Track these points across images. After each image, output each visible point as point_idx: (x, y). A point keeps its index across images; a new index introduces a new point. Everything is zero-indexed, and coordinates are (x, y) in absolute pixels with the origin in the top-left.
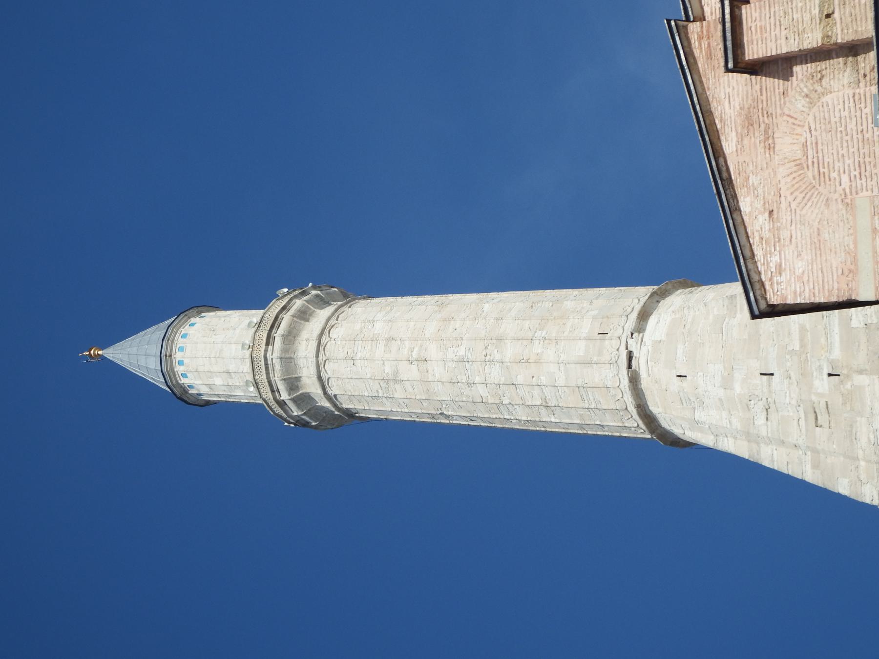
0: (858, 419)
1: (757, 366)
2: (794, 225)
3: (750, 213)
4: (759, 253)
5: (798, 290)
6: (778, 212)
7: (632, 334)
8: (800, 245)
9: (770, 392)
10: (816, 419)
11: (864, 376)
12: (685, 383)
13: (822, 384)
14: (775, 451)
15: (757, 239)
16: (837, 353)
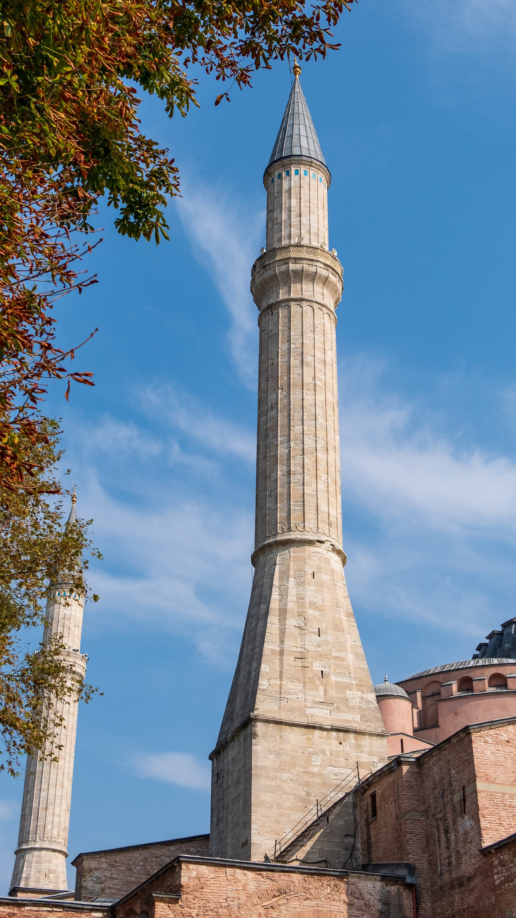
0: (301, 685)
1: (323, 627)
2: (503, 753)
3: (507, 730)
4: (492, 732)
5: (478, 750)
6: (509, 746)
7: (332, 545)
8: (496, 754)
9: (311, 633)
10: (299, 658)
11: (323, 693)
12: (310, 577)
13: (317, 666)
14: (276, 626)
15: (498, 732)
16: (333, 678)
